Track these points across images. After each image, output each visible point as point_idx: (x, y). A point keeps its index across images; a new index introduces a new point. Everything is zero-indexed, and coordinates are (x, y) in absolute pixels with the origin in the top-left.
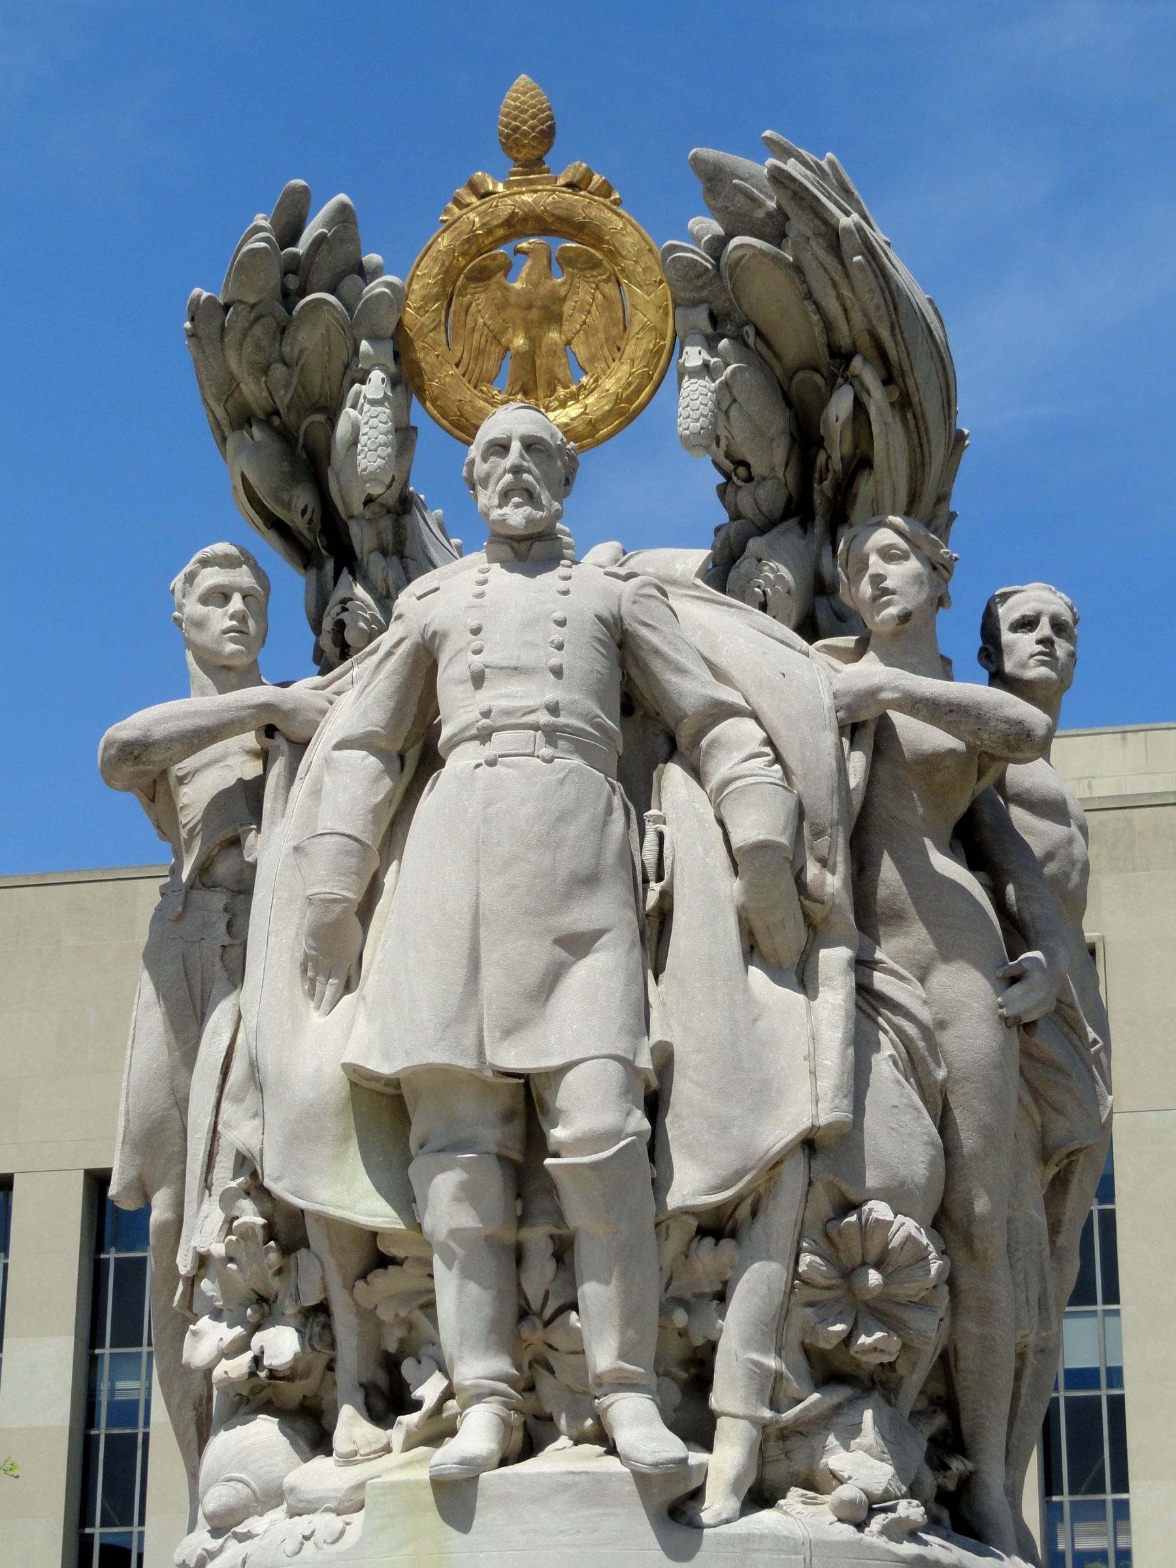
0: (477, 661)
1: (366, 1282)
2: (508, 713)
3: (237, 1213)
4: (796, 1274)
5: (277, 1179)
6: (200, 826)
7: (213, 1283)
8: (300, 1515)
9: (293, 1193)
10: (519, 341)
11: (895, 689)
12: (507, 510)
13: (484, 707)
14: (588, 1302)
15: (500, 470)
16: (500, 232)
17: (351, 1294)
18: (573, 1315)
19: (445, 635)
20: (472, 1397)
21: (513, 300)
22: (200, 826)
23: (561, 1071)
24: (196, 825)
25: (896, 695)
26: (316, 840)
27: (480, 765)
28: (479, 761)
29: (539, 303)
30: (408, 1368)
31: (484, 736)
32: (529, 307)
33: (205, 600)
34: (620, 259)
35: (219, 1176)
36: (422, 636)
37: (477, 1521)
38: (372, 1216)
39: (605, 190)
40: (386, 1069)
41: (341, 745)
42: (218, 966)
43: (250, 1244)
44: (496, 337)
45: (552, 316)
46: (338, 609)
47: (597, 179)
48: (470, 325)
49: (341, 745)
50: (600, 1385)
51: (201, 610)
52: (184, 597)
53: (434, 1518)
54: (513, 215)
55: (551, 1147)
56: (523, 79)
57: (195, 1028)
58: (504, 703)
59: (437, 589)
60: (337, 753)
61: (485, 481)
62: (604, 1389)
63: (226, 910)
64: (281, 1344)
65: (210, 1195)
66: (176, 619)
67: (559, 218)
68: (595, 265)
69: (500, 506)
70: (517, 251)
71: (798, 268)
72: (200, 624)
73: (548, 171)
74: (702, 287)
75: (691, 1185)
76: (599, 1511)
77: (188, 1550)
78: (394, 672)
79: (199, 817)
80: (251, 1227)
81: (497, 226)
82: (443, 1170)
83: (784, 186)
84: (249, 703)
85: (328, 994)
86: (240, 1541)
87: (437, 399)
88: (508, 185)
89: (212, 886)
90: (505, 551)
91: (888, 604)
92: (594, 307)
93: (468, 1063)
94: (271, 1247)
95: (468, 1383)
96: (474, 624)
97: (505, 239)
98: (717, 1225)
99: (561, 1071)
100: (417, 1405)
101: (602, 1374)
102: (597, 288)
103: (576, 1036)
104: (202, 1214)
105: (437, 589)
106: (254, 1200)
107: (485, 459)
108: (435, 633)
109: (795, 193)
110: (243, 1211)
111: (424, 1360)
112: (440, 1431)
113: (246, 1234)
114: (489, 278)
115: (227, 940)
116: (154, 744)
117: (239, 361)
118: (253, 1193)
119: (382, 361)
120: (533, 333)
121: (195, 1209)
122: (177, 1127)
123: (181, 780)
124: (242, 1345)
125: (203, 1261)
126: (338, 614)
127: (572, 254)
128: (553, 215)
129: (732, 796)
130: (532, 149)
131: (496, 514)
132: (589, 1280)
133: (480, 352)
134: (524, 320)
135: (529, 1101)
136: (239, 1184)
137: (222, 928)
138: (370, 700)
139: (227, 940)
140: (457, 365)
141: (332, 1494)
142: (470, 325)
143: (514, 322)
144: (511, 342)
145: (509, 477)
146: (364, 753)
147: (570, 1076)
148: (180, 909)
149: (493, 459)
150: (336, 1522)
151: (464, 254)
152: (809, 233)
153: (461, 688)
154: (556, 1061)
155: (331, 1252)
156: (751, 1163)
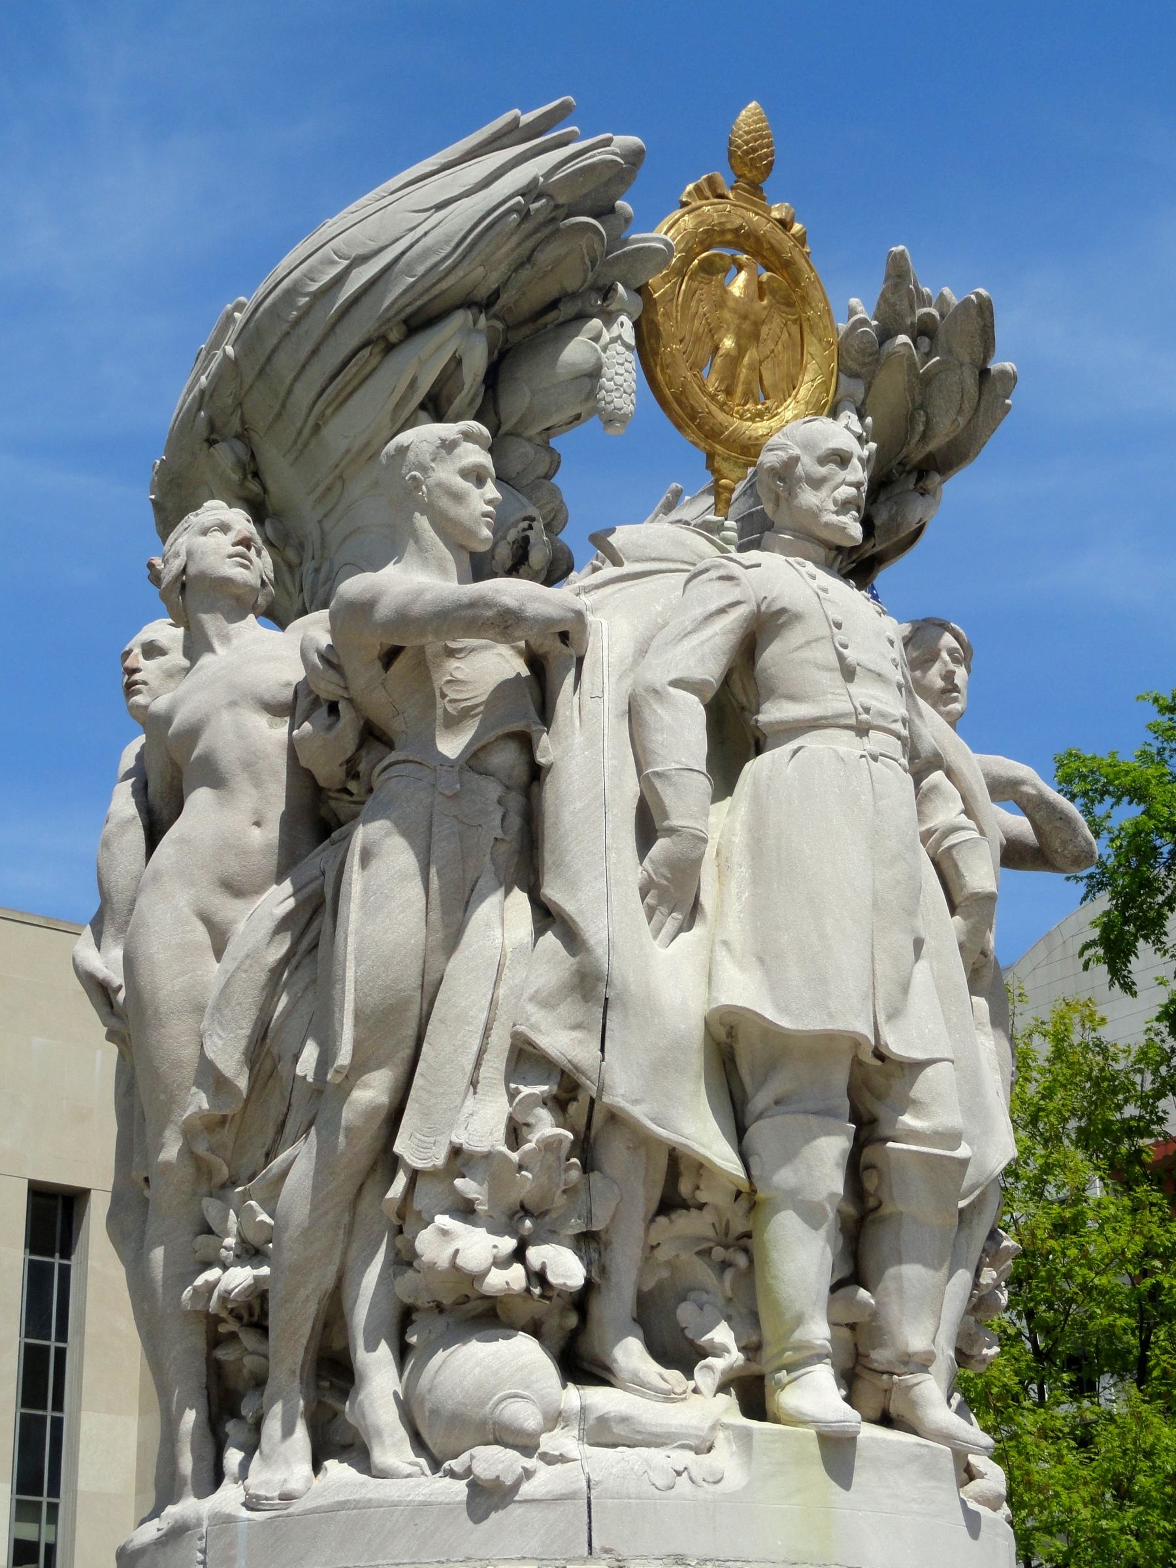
1: (671, 1221)
2: (883, 715)
3: (531, 1120)
4: (976, 1285)
5: (636, 1102)
6: (482, 708)
7: (481, 1184)
8: (628, 1446)
9: (652, 1120)
10: (728, 343)
11: (1034, 786)
12: (842, 518)
13: (869, 702)
14: (906, 1284)
15: (839, 479)
16: (729, 237)
17: (647, 1228)
18: (863, 1293)
20: (811, 1357)
21: (731, 304)
22: (482, 708)
23: (918, 1066)
24: (477, 706)
25: (1034, 792)
26: (686, 773)
27: (862, 756)
28: (864, 753)
29: (752, 317)
30: (686, 1313)
32: (745, 317)
33: (465, 473)
34: (808, 308)
35: (487, 1075)
36: (759, 606)
37: (856, 1479)
38: (723, 1159)
39: (801, 240)
40: (785, 1022)
41: (676, 683)
42: (488, 857)
43: (549, 1155)
44: (711, 332)
45: (755, 336)
46: (525, 524)
47: (797, 227)
48: (693, 310)
49: (676, 683)
50: (906, 1363)
51: (460, 483)
52: (433, 460)
53: (818, 1472)
54: (741, 227)
56: (753, 104)
57: (460, 914)
58: (874, 704)
59: (759, 565)
60: (671, 690)
61: (817, 483)
62: (912, 1367)
63: (500, 802)
64: (566, 1267)
65: (475, 1093)
66: (414, 478)
67: (772, 248)
68: (789, 304)
69: (837, 513)
70: (734, 261)
71: (926, 381)
72: (458, 497)
73: (764, 199)
74: (864, 365)
76: (933, 1483)
77: (500, 1466)
78: (732, 631)
79: (484, 698)
80: (559, 1140)
81: (730, 230)
82: (828, 1133)
83: (983, 319)
84: (571, 606)
85: (670, 925)
86: (549, 1463)
87: (668, 366)
88: (738, 196)
89: (486, 773)
90: (822, 552)
91: (955, 700)
92: (780, 343)
94: (574, 1164)
95: (819, 1342)
96: (839, 618)
97: (728, 244)
99: (918, 1066)
101: (916, 1354)
102: (785, 325)
104: (466, 1110)
105: (759, 565)
106: (550, 1110)
107: (823, 461)
108: (783, 611)
109: (985, 325)
110: (540, 1120)
111: (707, 1308)
113: (549, 1145)
114: (712, 274)
115: (498, 833)
116: (525, 619)
117: (513, 250)
118: (549, 1104)
119: (631, 309)
120: (743, 342)
121: (459, 1100)
122: (415, 1010)
123: (451, 653)
124: (519, 1255)
125: (459, 1159)
126: (524, 530)
127: (775, 285)
128: (769, 242)
129: (969, 844)
130: (753, 172)
131: (834, 518)
132: (906, 1263)
133: (698, 339)
134: (739, 327)
136: (542, 1092)
137: (498, 821)
138: (706, 649)
139: (498, 833)
140: (681, 341)
141: (692, 1432)
142: (693, 310)
143: (728, 325)
144: (721, 340)
146: (697, 699)
147: (929, 1071)
148: (458, 786)
149: (832, 466)
151: (701, 242)
152: (967, 359)
153: (828, 675)
154: (918, 1055)
155: (644, 1184)
156: (982, 1179)
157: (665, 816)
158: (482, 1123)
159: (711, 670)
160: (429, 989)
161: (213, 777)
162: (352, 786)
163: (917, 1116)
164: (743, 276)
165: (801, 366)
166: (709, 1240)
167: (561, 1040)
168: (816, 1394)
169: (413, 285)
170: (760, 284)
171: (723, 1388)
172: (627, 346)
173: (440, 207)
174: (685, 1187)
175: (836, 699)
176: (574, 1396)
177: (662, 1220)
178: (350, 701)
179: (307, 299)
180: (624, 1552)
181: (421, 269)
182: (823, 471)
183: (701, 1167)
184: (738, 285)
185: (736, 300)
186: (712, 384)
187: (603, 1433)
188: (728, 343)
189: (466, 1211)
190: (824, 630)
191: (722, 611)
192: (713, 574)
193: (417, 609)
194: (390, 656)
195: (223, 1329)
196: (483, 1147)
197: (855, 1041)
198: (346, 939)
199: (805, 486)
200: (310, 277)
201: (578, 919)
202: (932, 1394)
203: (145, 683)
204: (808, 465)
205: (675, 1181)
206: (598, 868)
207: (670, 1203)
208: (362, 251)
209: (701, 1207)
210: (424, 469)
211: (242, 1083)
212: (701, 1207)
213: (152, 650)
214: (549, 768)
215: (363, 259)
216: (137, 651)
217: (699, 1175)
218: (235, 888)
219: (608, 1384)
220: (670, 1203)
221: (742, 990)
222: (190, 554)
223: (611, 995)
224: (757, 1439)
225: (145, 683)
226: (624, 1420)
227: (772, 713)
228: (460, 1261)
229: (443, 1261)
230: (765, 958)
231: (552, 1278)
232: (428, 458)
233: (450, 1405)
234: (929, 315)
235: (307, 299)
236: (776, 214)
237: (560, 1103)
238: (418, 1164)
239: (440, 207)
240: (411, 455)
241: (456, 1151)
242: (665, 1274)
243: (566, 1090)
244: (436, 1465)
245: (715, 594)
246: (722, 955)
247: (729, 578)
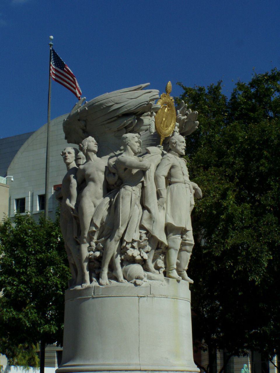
10: (164, 119)
23: (189, 231)
40: (176, 225)
41: (162, 176)
56: (170, 82)
96: (183, 167)
99: (189, 231)
108: (175, 165)
125: (133, 241)
157: (161, 195)
158: (136, 237)
159: (166, 174)
160: (130, 217)
161: (93, 180)
162: (115, 186)
163: (188, 238)
164: (166, 109)
165: (172, 122)
166: (160, 253)
167: (146, 225)
168: (175, 274)
169: (127, 111)
170: (168, 110)
172: (154, 121)
173: (131, 99)
174: (159, 246)
175: (182, 180)
176: (147, 273)
177: (157, 250)
178: (118, 174)
179: (105, 107)
180: (155, 294)
181: (128, 109)
183: (162, 243)
184: (166, 110)
185: (166, 112)
186: (162, 125)
187: (150, 278)
188: (164, 119)
189: (133, 247)
190: (180, 168)
192: (166, 159)
193: (133, 165)
194: (126, 169)
195: (92, 260)
196: (137, 240)
197: (183, 228)
198: (120, 210)
199: (178, 146)
200: (106, 103)
201: (151, 209)
202: (185, 274)
203: (69, 158)
204: (178, 143)
206: (153, 202)
207: (158, 248)
208: (117, 102)
209: (161, 248)
210: (130, 141)
211: (99, 227)
212: (161, 248)
213: (69, 153)
214: (145, 187)
215: (117, 103)
216: (67, 153)
217: (162, 245)
218: (97, 198)
219: (148, 272)
220: (158, 248)
221: (170, 221)
222: (88, 146)
223: (155, 220)
224: (170, 280)
225: (69, 158)
226: (153, 277)
227: (173, 180)
228: (134, 255)
229: (131, 255)
230: (173, 216)
231: (144, 257)
232: (131, 139)
233: (131, 274)
234: (187, 113)
235: (105, 107)
236: (171, 99)
237: (146, 234)
238: (128, 241)
239: (131, 99)
240: (128, 138)
241: (133, 240)
243: (148, 233)
244: (128, 281)
246: (167, 215)
247: (169, 160)
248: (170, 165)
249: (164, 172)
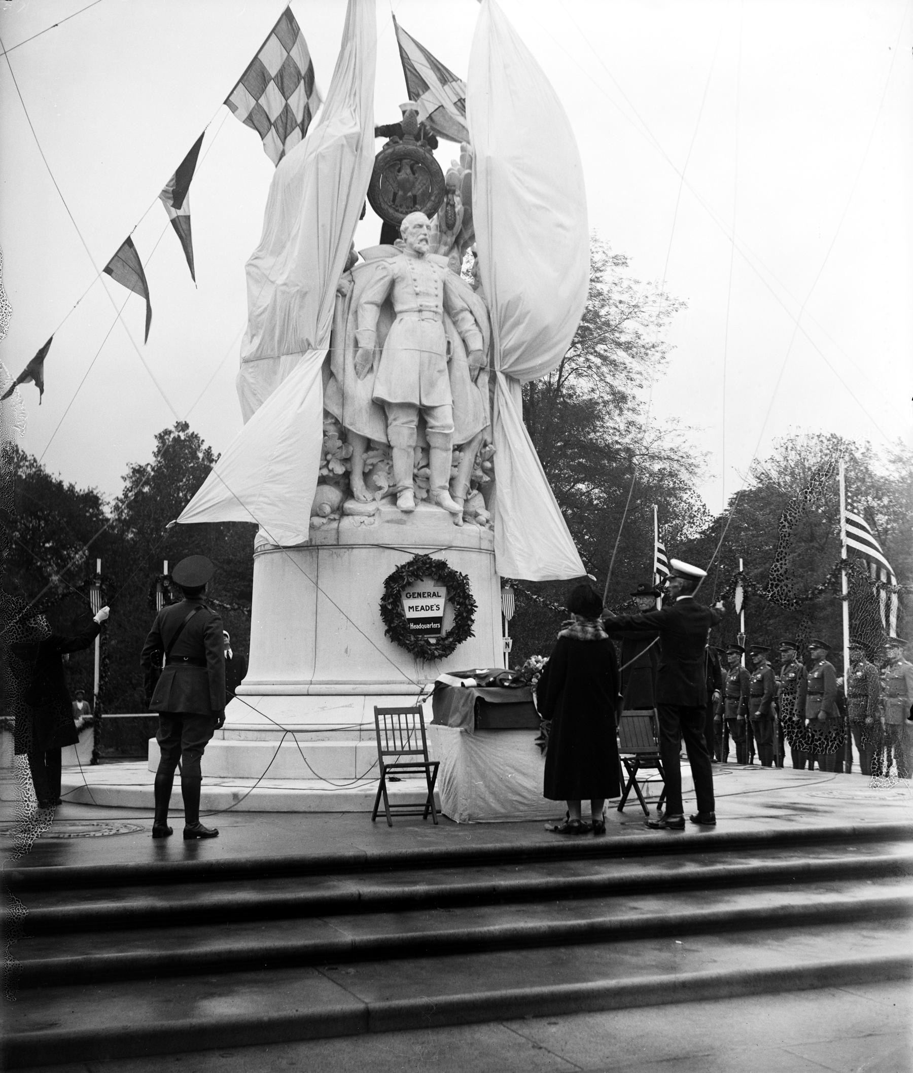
0: (418, 290)
19: (403, 279)
31: (420, 311)
41: (366, 303)
49: (366, 303)
55: (430, 425)
75: (458, 440)
93: (418, 403)
98: (459, 448)
100: (380, 488)
103: (440, 397)
107: (414, 227)
112: (393, 497)
135: (423, 413)
145: (422, 237)
147: (440, 409)
150: (372, 519)
171: (382, 498)
182: (415, 231)
191: (382, 279)
205: (369, 444)
209: (377, 450)
242: (371, 467)
245: (380, 273)
248: (387, 280)
249: (377, 293)
